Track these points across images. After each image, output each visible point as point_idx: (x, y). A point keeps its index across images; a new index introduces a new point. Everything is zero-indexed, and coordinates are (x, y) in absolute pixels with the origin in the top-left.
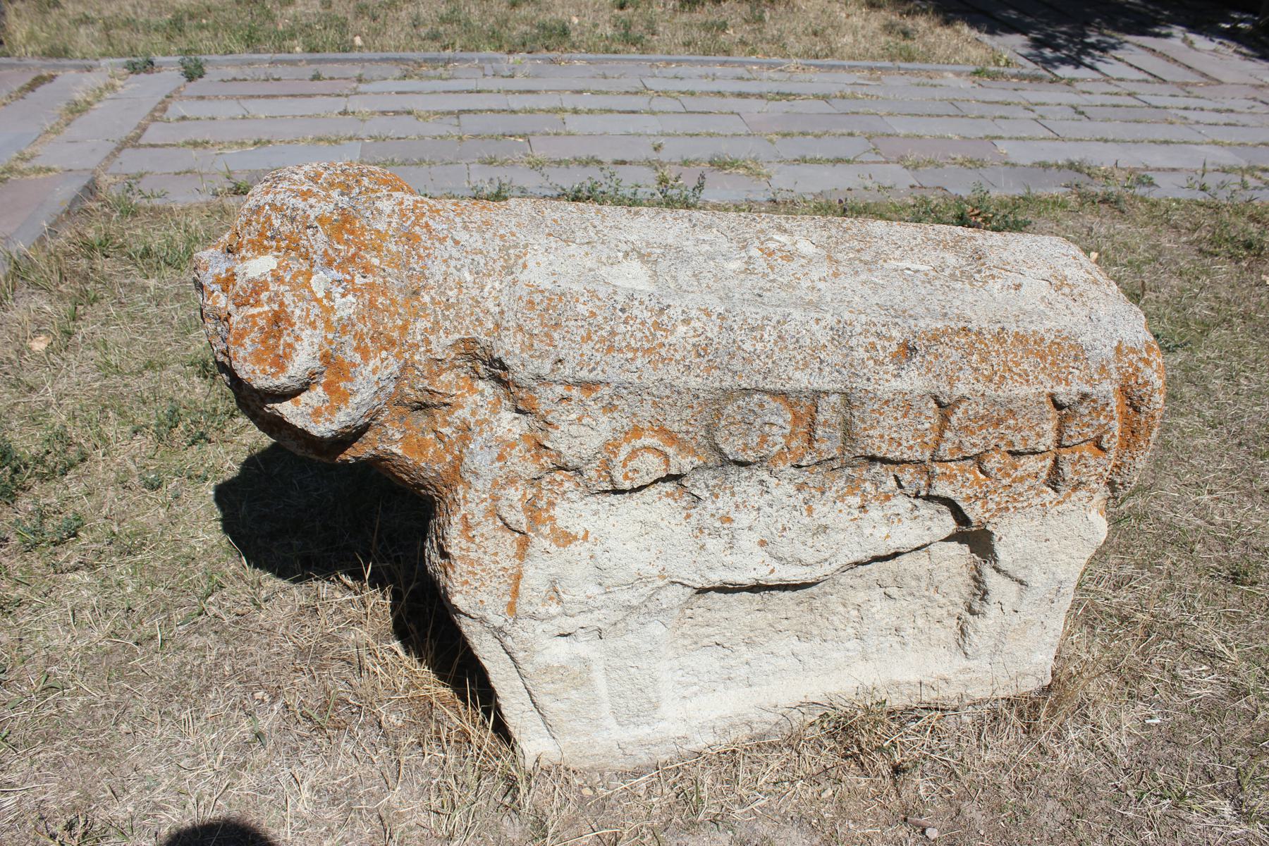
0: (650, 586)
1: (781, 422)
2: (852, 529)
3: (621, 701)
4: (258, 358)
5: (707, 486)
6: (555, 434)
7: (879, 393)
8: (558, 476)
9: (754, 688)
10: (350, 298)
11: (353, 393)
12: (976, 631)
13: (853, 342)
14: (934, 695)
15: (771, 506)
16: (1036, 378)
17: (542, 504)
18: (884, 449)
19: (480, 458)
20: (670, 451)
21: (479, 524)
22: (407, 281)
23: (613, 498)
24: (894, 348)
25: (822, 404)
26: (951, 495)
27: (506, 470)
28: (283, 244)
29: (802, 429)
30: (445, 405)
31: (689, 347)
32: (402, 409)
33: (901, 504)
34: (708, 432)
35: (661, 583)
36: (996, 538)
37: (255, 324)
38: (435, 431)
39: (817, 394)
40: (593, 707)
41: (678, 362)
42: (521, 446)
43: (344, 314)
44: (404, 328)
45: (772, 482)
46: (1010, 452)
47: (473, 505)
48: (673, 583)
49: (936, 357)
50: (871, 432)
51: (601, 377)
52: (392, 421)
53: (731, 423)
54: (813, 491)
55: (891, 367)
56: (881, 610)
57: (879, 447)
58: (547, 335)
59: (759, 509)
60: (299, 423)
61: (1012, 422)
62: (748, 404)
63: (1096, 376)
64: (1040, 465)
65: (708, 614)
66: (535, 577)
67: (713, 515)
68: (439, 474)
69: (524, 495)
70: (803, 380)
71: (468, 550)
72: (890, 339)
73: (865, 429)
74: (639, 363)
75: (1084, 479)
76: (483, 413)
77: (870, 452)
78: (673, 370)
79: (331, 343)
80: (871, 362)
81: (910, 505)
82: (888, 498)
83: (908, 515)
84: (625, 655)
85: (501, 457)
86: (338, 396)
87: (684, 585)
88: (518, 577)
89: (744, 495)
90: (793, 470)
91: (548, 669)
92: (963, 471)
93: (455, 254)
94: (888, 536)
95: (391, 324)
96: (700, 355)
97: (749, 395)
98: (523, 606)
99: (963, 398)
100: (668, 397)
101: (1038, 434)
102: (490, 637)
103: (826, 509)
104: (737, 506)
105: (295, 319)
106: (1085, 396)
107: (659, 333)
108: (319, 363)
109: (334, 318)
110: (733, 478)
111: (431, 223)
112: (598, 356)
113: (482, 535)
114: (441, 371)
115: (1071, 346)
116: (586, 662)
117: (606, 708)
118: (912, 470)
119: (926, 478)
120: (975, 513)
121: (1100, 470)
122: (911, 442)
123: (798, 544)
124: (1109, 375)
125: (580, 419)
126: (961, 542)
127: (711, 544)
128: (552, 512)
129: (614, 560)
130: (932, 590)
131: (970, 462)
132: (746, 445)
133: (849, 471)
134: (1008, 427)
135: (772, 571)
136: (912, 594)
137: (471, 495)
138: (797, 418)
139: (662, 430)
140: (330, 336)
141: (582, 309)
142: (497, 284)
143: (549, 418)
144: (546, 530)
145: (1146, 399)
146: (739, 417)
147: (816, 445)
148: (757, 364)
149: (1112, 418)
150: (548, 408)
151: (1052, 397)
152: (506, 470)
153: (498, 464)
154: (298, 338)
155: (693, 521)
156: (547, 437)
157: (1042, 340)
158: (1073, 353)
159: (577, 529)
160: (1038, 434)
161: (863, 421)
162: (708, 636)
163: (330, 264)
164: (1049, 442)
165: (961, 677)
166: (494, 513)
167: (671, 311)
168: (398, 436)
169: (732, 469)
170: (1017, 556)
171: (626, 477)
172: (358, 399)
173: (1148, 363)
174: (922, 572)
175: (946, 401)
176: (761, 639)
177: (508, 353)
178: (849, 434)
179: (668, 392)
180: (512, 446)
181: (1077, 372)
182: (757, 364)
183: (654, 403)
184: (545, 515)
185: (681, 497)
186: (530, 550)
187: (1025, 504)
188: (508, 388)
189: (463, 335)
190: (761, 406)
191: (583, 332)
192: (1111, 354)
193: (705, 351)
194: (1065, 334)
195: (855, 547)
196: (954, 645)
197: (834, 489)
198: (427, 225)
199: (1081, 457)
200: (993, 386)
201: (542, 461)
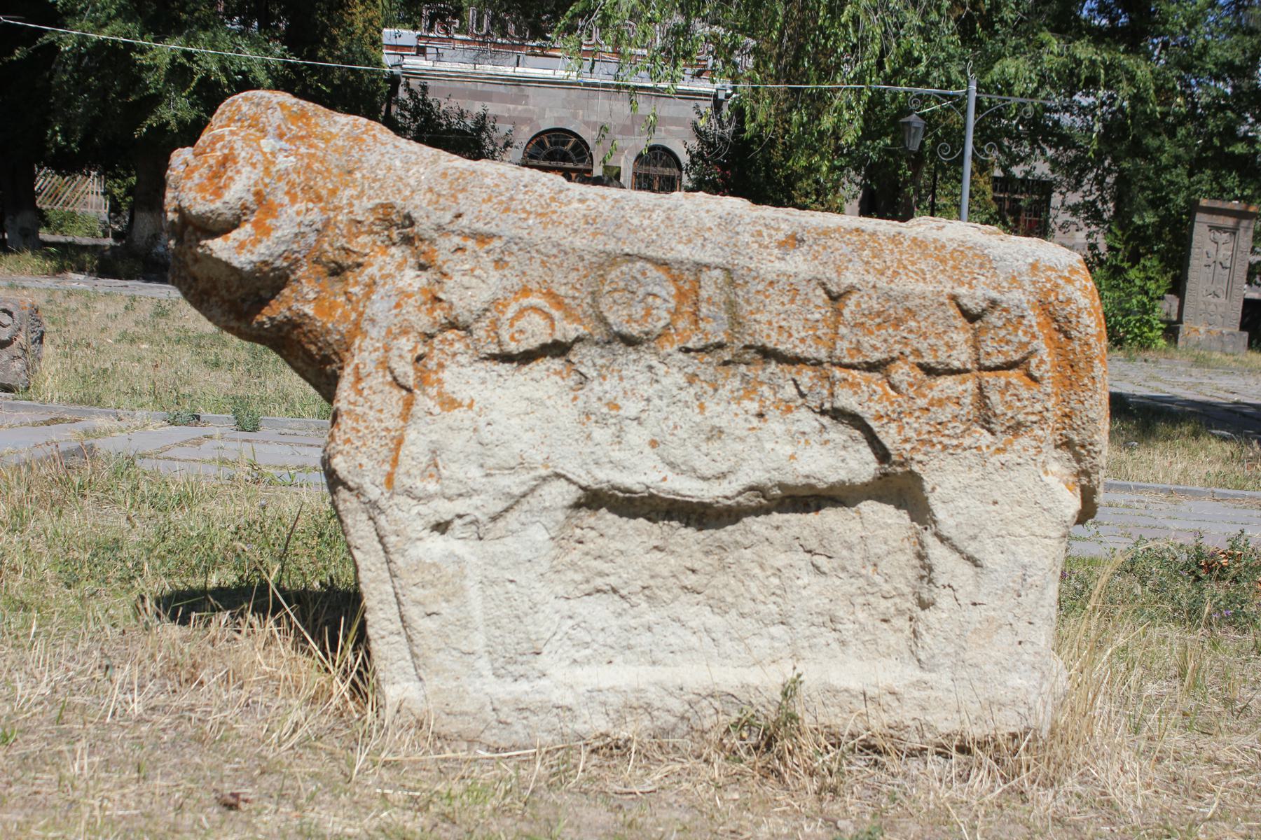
0: (533, 474)
1: (664, 293)
2: (751, 440)
3: (497, 633)
4: (201, 188)
5: (594, 365)
6: (449, 284)
7: (762, 272)
8: (450, 335)
9: (657, 668)
10: (292, 158)
11: (277, 228)
12: (928, 628)
13: (740, 229)
14: (885, 718)
15: (661, 398)
16: (935, 277)
17: (432, 364)
18: (774, 341)
19: (379, 306)
20: (556, 314)
21: (369, 375)
22: (344, 162)
23: (504, 368)
24: (781, 236)
25: (705, 277)
26: (859, 410)
27: (400, 318)
28: (246, 124)
29: (687, 308)
30: (359, 265)
31: (579, 216)
32: (320, 268)
33: (807, 420)
34: (594, 300)
35: (544, 472)
36: (928, 487)
37: (206, 162)
38: (346, 293)
39: (700, 267)
40: (464, 633)
41: (567, 226)
42: (419, 298)
43: (282, 167)
44: (333, 192)
45: (661, 369)
46: (920, 366)
47: (366, 354)
48: (559, 476)
49: (824, 248)
50: (758, 317)
51: (494, 230)
52: (308, 278)
53: (615, 290)
54: (704, 385)
55: (776, 251)
56: (811, 592)
57: (768, 336)
58: (453, 196)
59: (648, 400)
60: (224, 256)
61: (913, 324)
62: (631, 270)
63: (1005, 284)
64: (961, 388)
65: (600, 541)
66: (417, 441)
67: (600, 399)
68: (342, 335)
69: (415, 348)
70: (684, 252)
71: (355, 404)
72: (778, 229)
73: (752, 313)
74: (531, 222)
75: (1021, 417)
76: (390, 269)
77: (760, 341)
78: (561, 232)
79: (266, 185)
80: (756, 246)
81: (816, 424)
82: (789, 410)
83: (816, 437)
84: (503, 563)
85: (398, 305)
86: (263, 230)
87: (568, 479)
88: (399, 442)
89: (633, 382)
90: (681, 356)
91: (419, 565)
92: (868, 382)
93: (392, 151)
94: (792, 457)
95: (323, 186)
96: (587, 223)
97: (632, 262)
98: (402, 480)
99: (850, 290)
100: (555, 256)
101: (947, 344)
102: (365, 517)
103: (719, 409)
104: (625, 393)
105: (240, 159)
106: (994, 304)
107: (553, 204)
108: (252, 198)
109: (274, 169)
110: (621, 360)
111: (379, 135)
112: (494, 214)
113: (370, 388)
114: (360, 233)
115: (976, 255)
116: (459, 560)
117: (479, 641)
118: (811, 373)
119: (827, 385)
120: (890, 437)
121: (1038, 407)
122: (803, 334)
123: (691, 449)
124: (1021, 286)
125: (472, 270)
126: (898, 507)
127: (599, 434)
128: (441, 375)
129: (497, 434)
130: (870, 568)
131: (877, 376)
132: (630, 316)
133: (743, 368)
134: (911, 331)
135: (665, 479)
136: (844, 569)
137: (367, 342)
138: (681, 295)
139: (550, 294)
140: (267, 180)
141: (488, 181)
142: (422, 170)
143: (445, 269)
144: (433, 391)
145: (1074, 319)
146: (622, 284)
147: (702, 325)
148: (642, 234)
149: (1034, 336)
150: (445, 258)
151: (954, 298)
152: (400, 318)
153: (394, 312)
154: (238, 172)
155: (580, 403)
156: (441, 289)
157: (943, 247)
158: (978, 261)
159: (463, 395)
160: (947, 344)
161: (748, 302)
162: (601, 574)
163: (281, 136)
164: (964, 358)
165: (916, 694)
166: (385, 365)
167: (570, 193)
168: (312, 296)
169: (618, 347)
170: (960, 519)
171: (512, 338)
172: (279, 233)
173: (1068, 280)
174: (854, 539)
175: (834, 289)
176: (665, 595)
177: (416, 207)
178: (736, 321)
179: (555, 251)
180: (409, 296)
181: (982, 279)
182: (642, 234)
183: (543, 262)
184: (434, 377)
185: (568, 375)
186: (415, 409)
187: (955, 442)
188: (413, 244)
189: (383, 200)
190: (644, 274)
191: (485, 196)
192: (1024, 268)
193: (594, 220)
194: (970, 244)
195: (757, 465)
196: (907, 655)
197: (728, 387)
198: (374, 136)
199: (1008, 384)
200: (884, 279)
201: (435, 314)
